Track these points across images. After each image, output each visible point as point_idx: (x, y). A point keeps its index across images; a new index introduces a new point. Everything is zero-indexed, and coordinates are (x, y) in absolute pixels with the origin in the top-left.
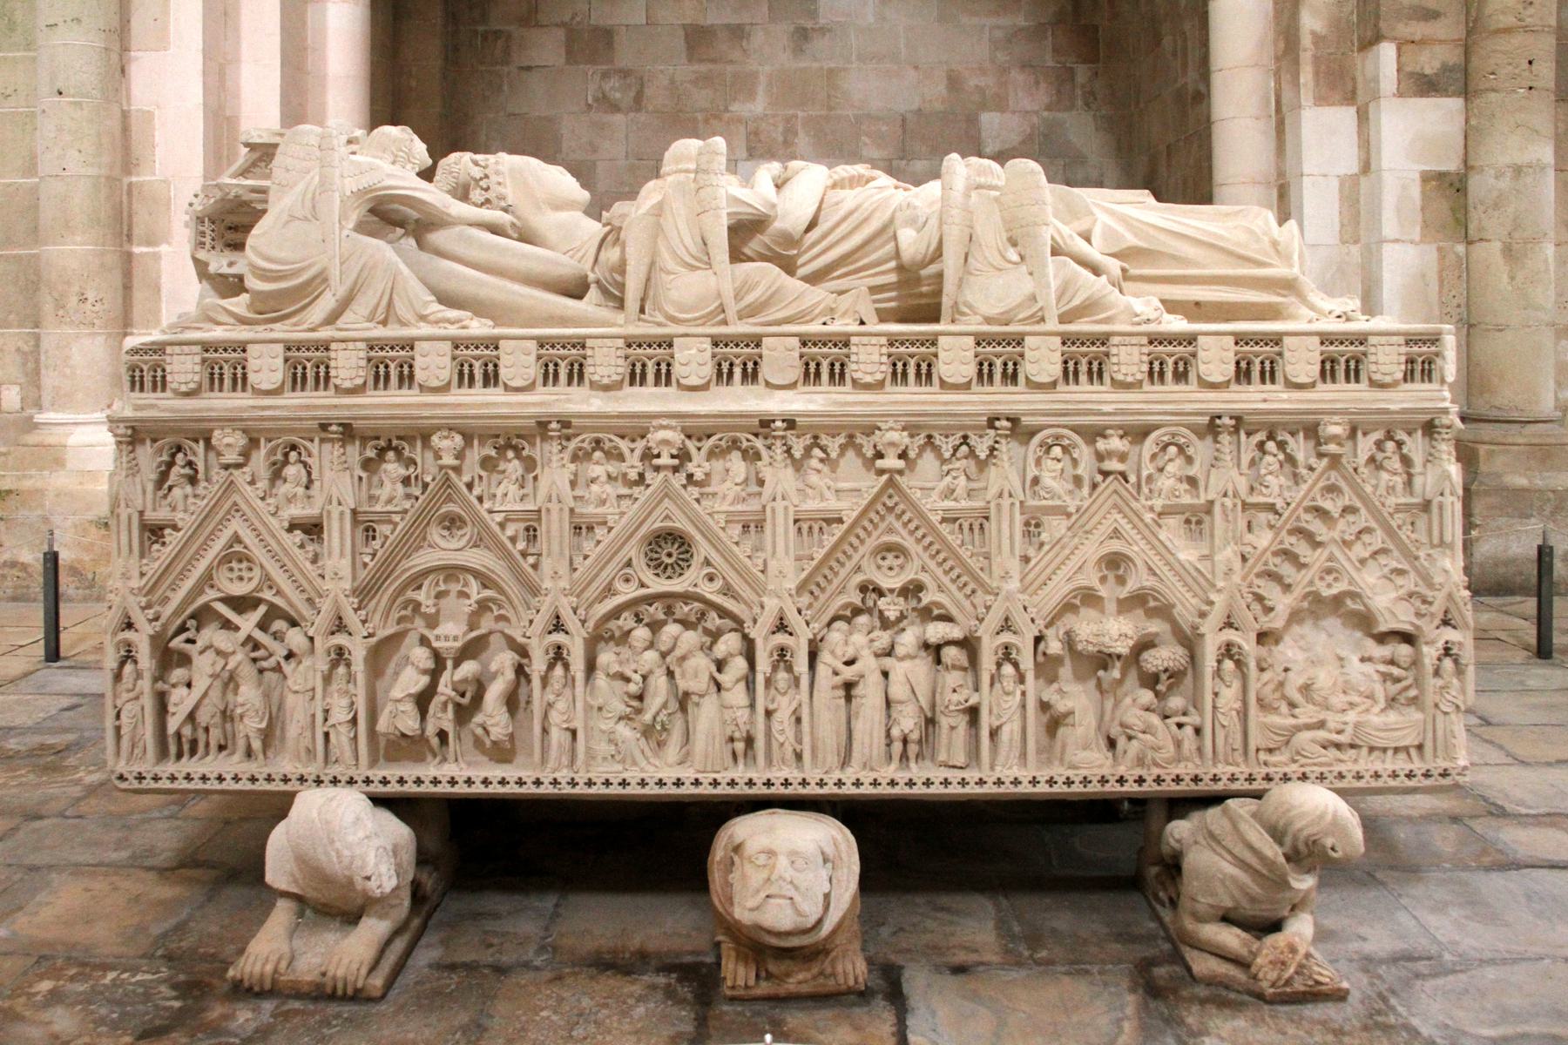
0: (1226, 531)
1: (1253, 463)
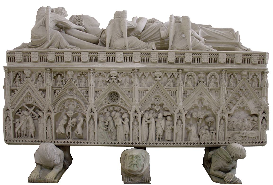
1: (229, 80)
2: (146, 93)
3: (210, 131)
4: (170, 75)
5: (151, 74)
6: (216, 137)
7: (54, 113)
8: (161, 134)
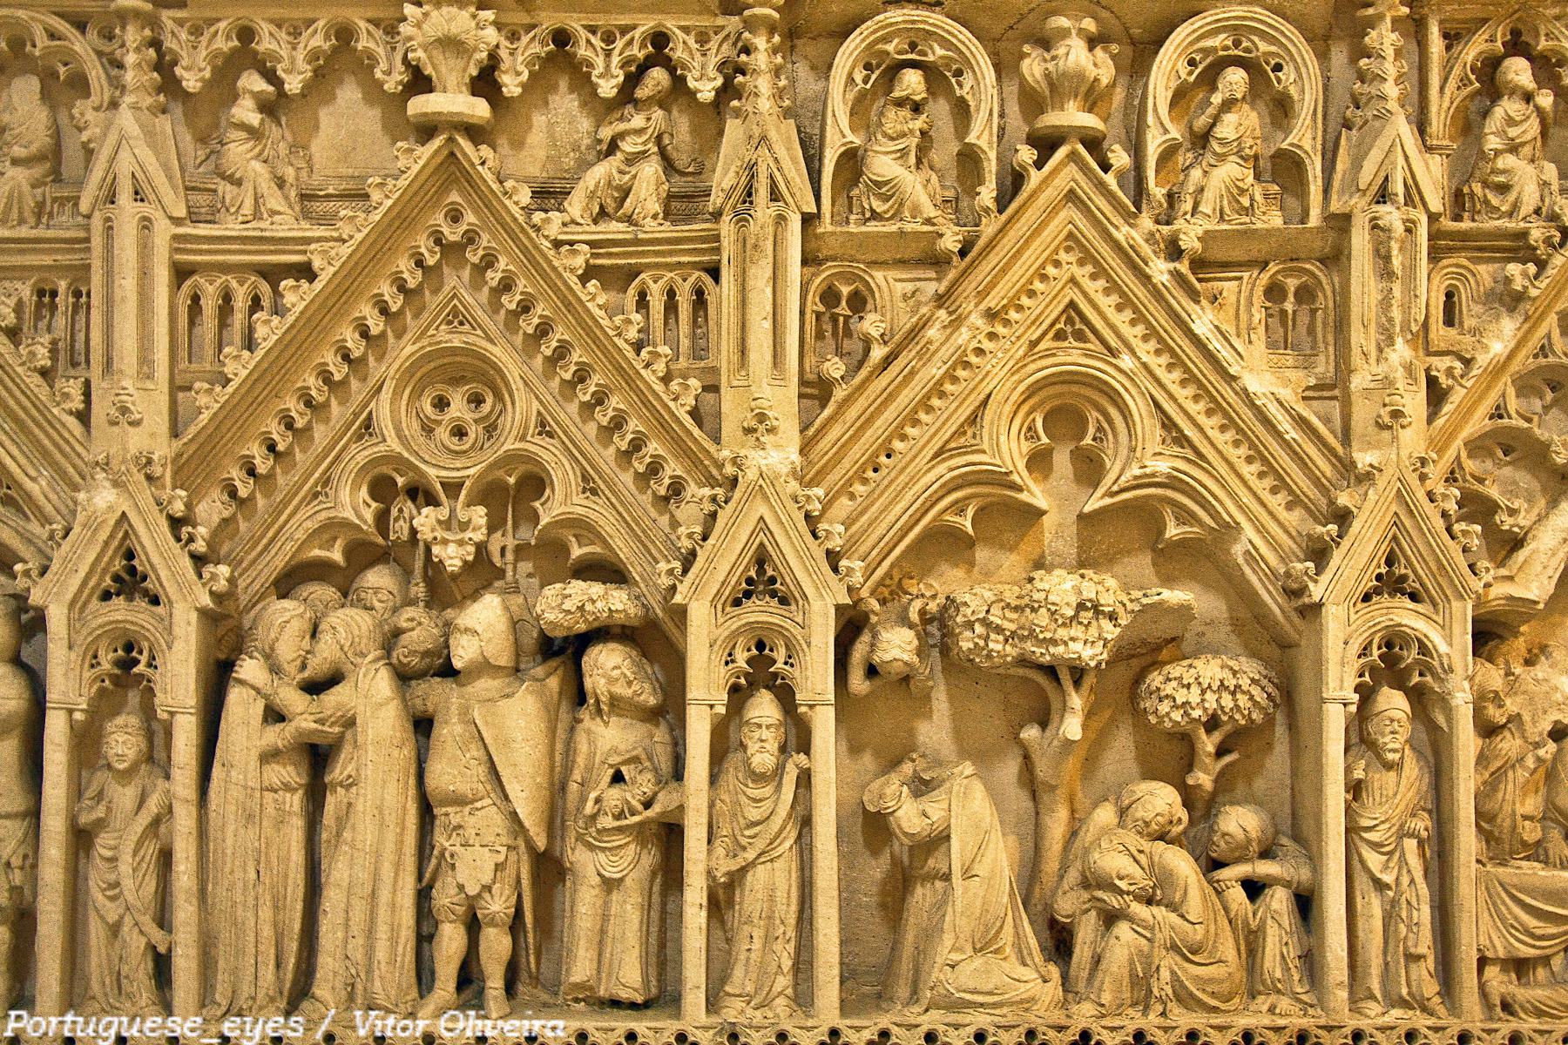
0: (1385, 303)
2: (279, 310)
3: (1217, 864)
4: (615, 60)
5: (363, 43)
6: (1311, 963)
8: (498, 905)
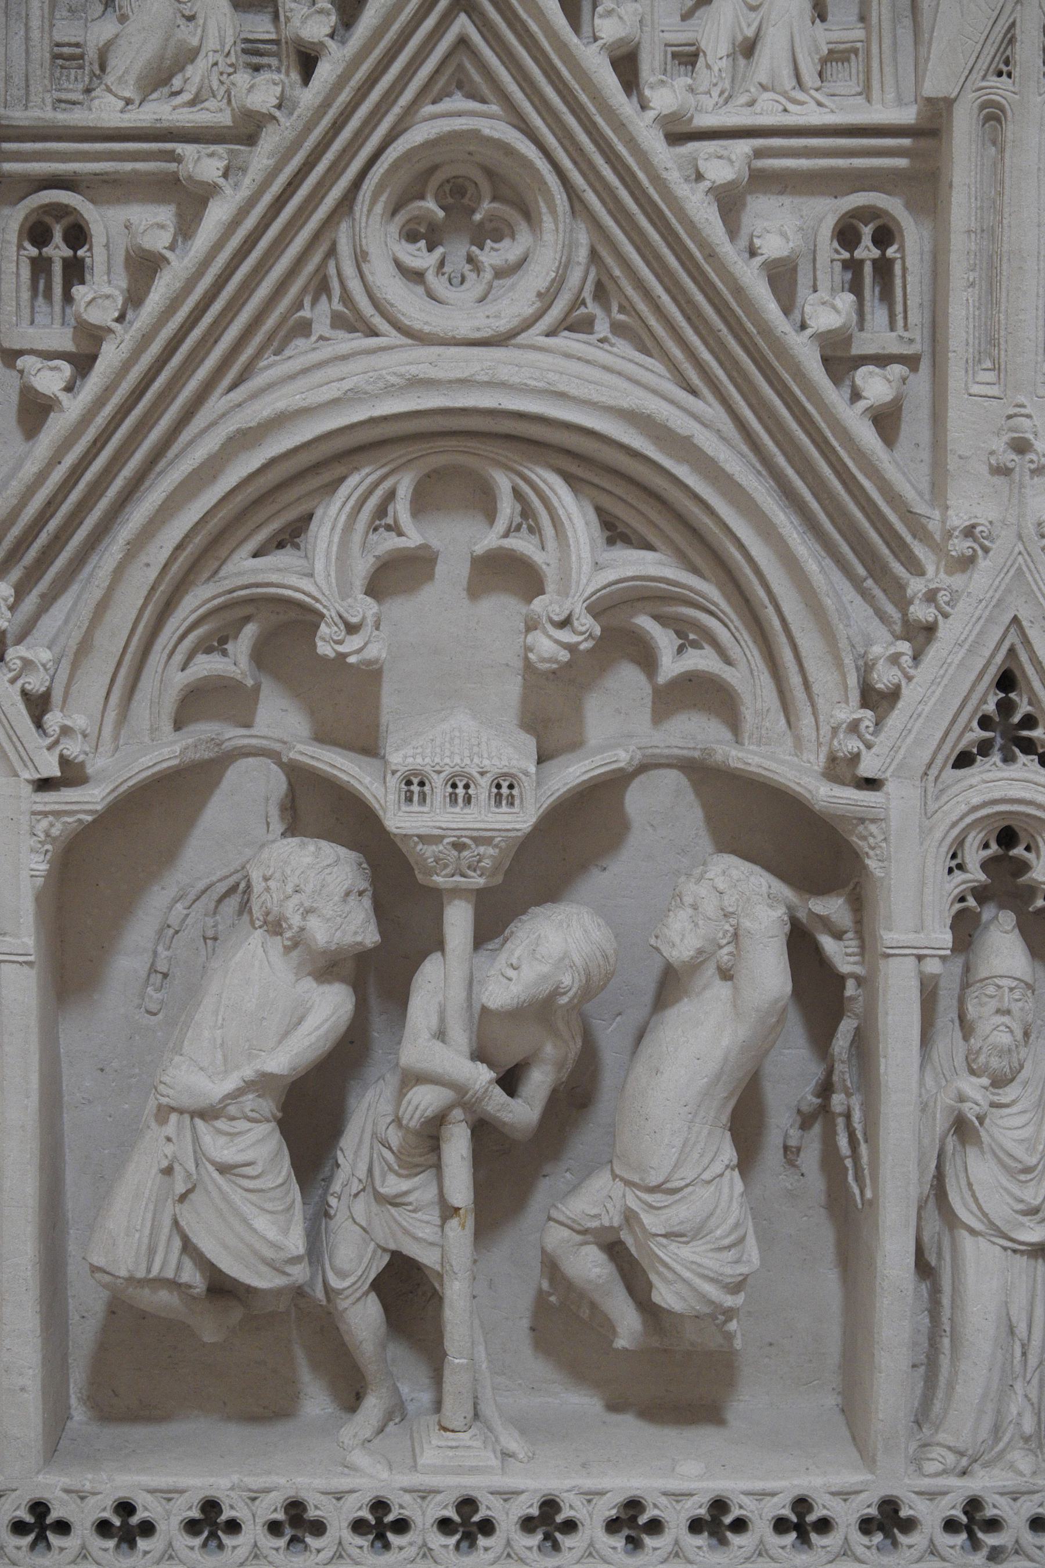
7: (44, 785)
